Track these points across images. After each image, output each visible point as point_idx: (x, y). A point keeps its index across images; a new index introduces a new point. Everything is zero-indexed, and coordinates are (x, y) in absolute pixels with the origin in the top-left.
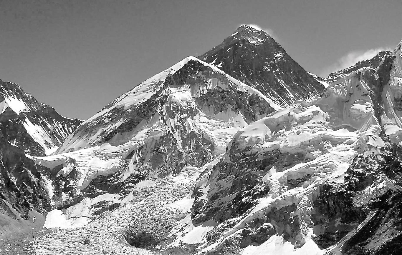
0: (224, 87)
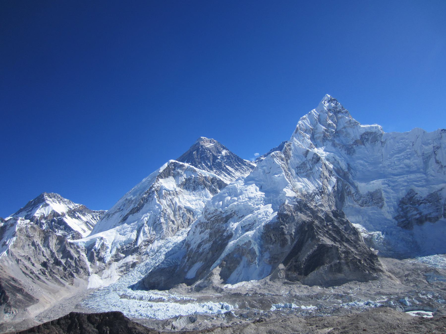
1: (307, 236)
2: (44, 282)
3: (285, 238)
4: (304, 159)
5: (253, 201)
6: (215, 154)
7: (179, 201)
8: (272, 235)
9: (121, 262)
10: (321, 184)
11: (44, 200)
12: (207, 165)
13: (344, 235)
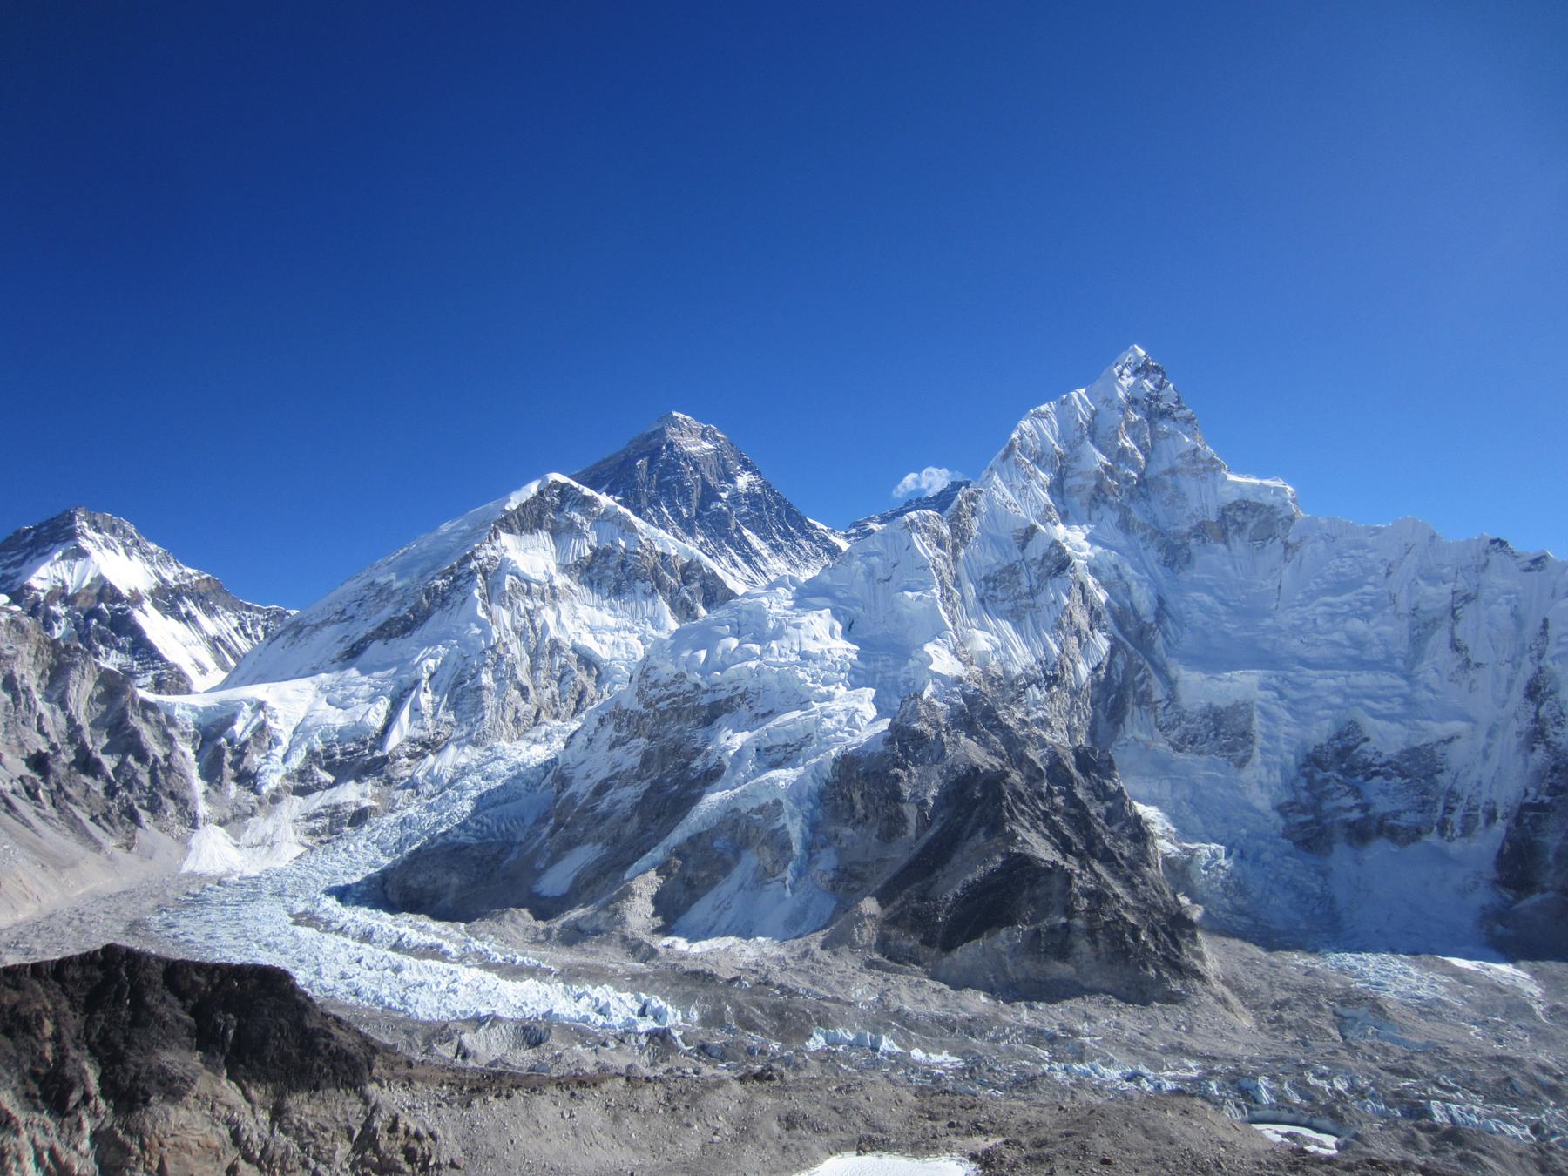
1: (973, 820)
2: (28, 824)
3: (900, 813)
4: (1016, 555)
5: (814, 667)
6: (713, 482)
7: (558, 621)
8: (857, 796)
9: (317, 801)
10: (1056, 650)
11: (72, 535)
12: (677, 514)
13: (1099, 837)
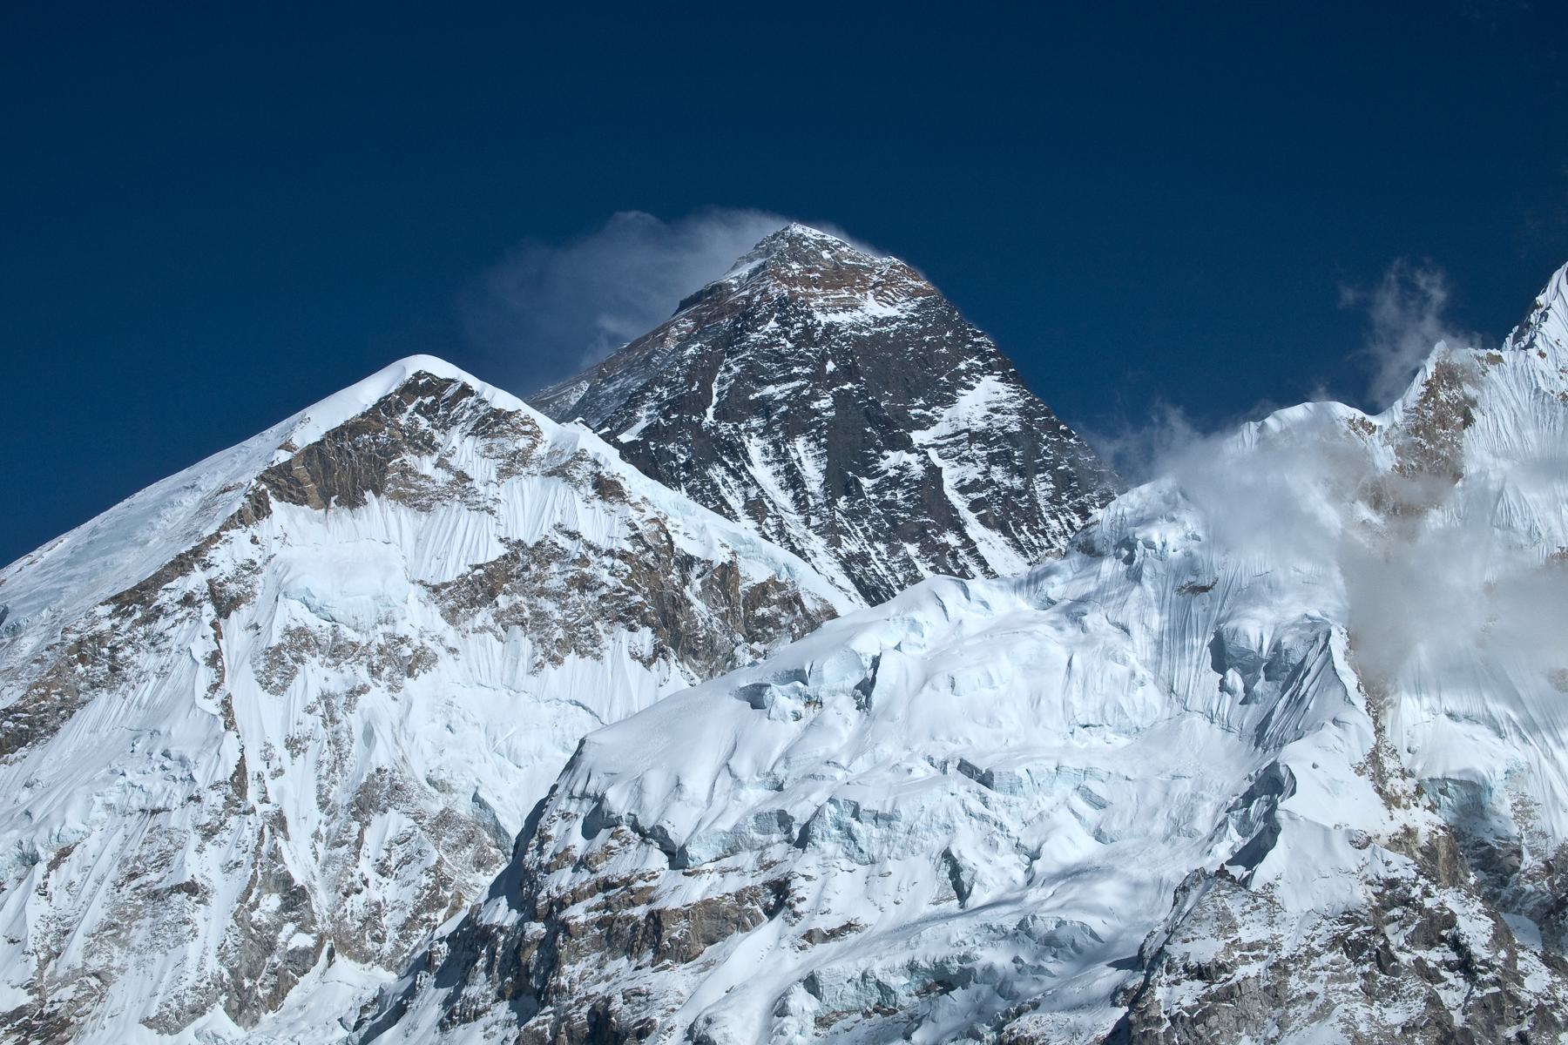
0: (598, 525)
12: (794, 480)
